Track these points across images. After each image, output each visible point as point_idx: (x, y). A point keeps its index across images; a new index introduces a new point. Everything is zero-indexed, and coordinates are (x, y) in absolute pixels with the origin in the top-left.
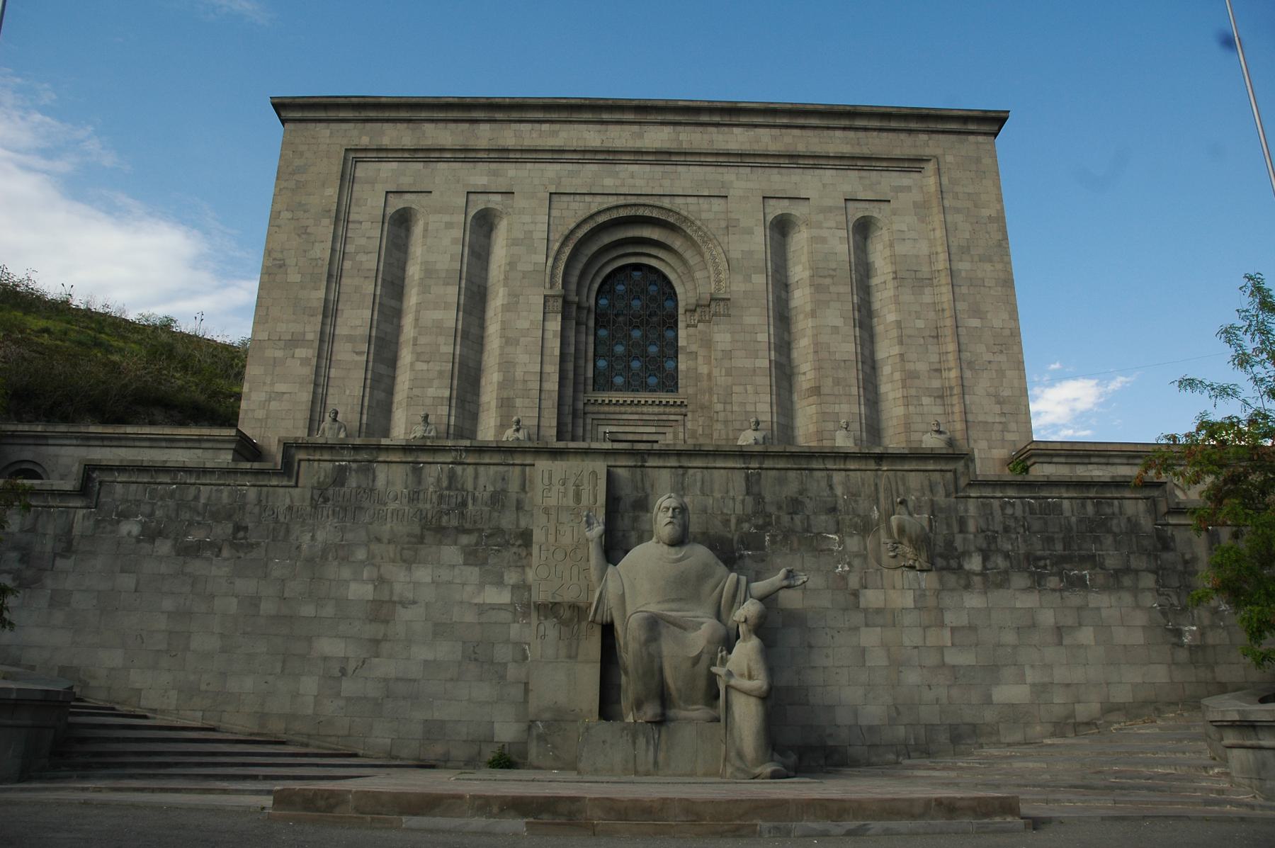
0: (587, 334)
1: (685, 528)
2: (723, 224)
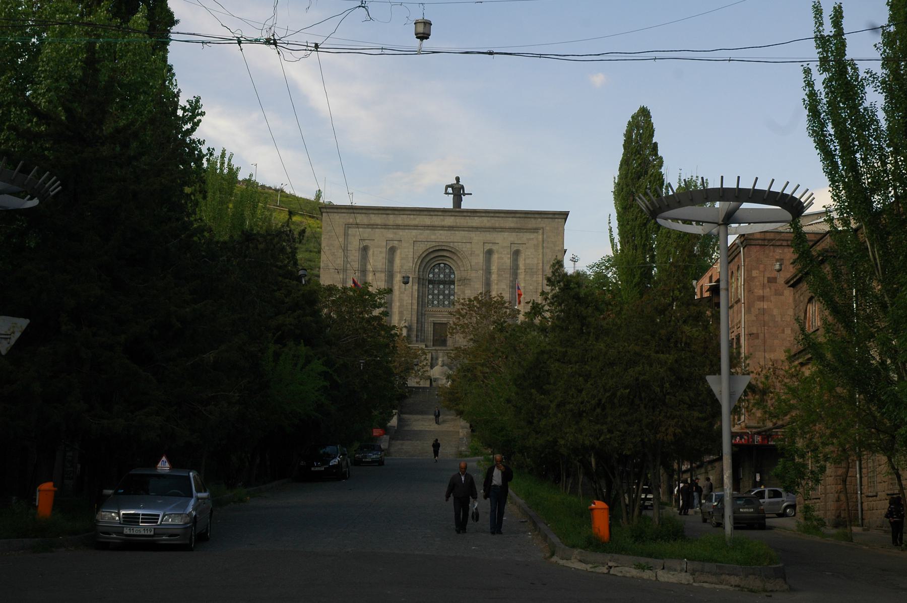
0: (426, 288)
1: (444, 364)
2: (470, 253)
